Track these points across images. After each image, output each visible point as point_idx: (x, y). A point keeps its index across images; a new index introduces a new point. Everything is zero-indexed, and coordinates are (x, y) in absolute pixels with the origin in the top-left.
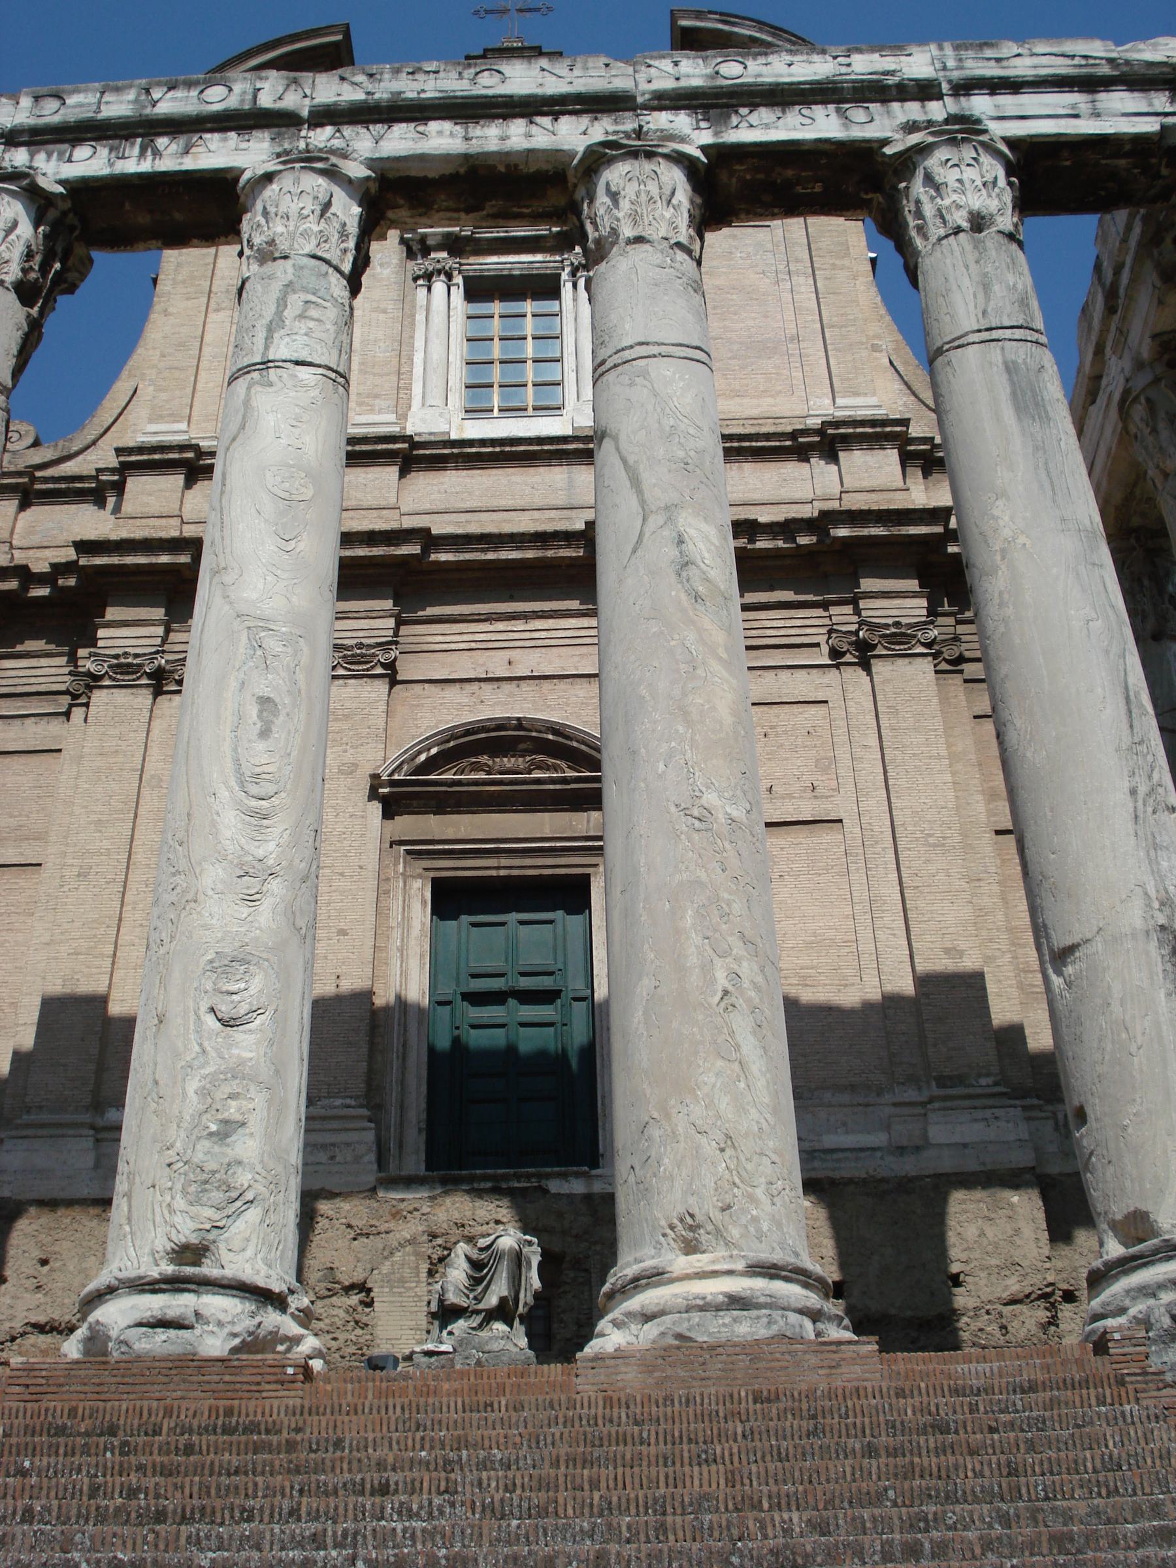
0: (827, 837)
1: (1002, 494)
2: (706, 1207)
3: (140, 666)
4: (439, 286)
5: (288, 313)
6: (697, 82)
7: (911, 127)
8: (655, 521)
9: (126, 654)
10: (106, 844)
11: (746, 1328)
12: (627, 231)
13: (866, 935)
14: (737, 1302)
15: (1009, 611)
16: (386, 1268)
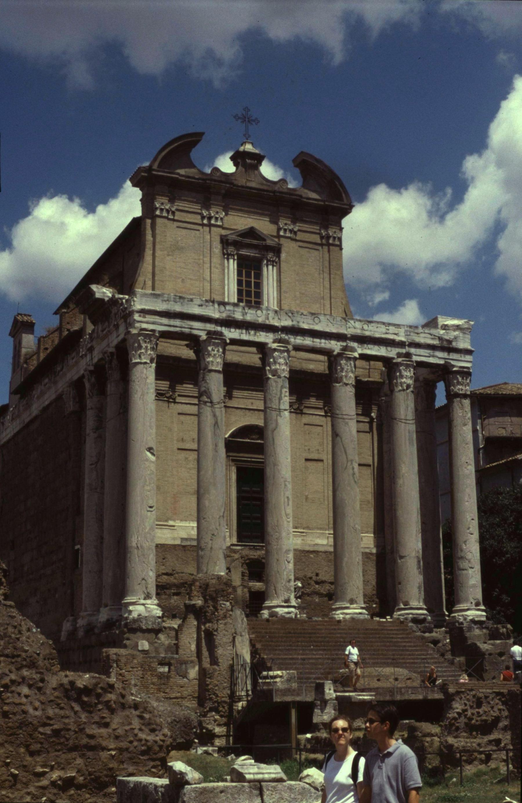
0: (320, 464)
1: (404, 463)
2: (354, 597)
3: (164, 394)
4: (231, 261)
5: (283, 395)
6: (358, 332)
7: (399, 355)
8: (349, 463)
9: (161, 390)
10: (162, 449)
11: (361, 617)
12: (345, 380)
13: (326, 491)
14: (360, 613)
15: (402, 489)
16: (233, 564)
